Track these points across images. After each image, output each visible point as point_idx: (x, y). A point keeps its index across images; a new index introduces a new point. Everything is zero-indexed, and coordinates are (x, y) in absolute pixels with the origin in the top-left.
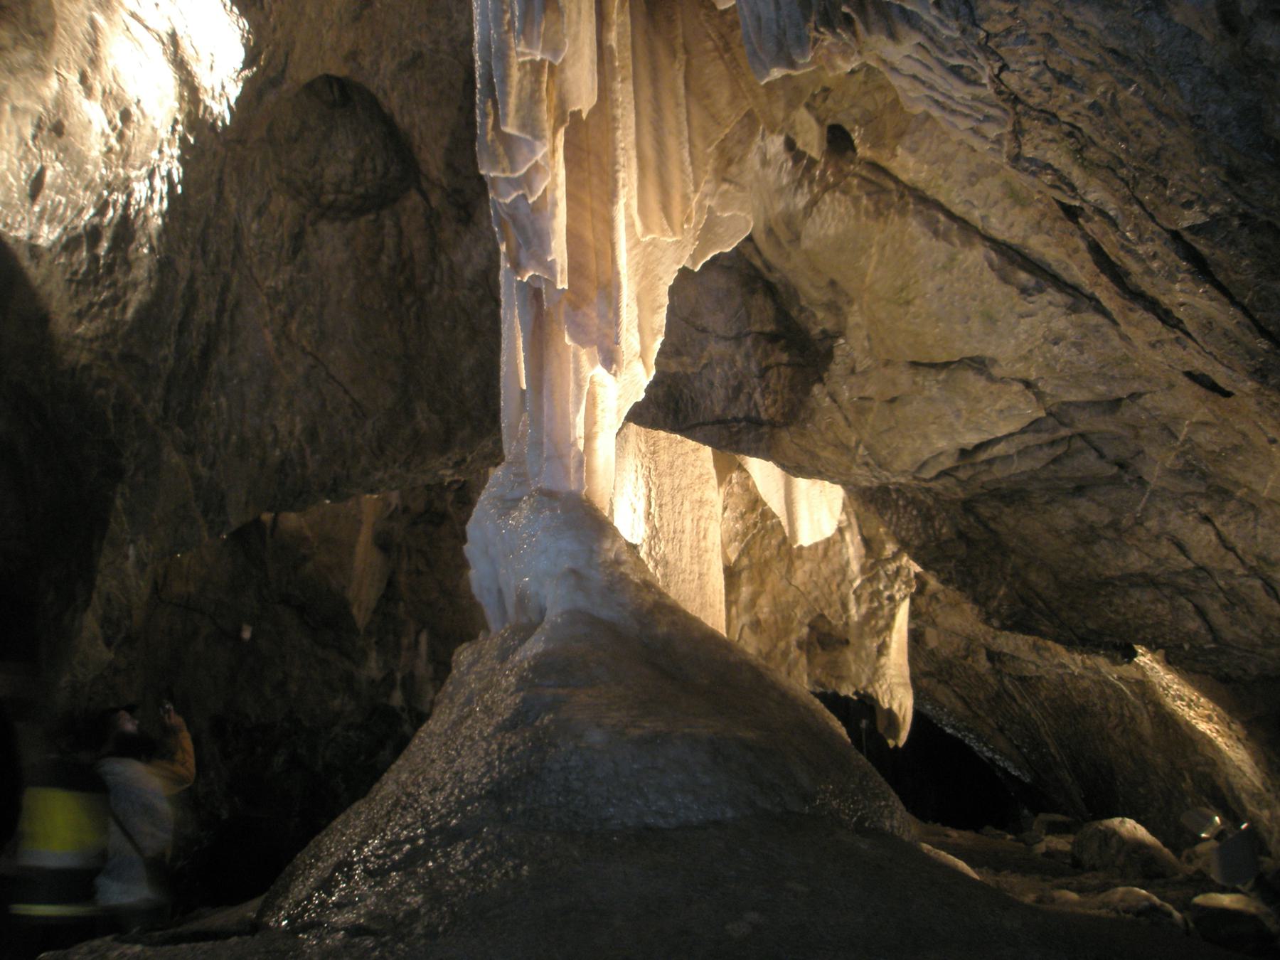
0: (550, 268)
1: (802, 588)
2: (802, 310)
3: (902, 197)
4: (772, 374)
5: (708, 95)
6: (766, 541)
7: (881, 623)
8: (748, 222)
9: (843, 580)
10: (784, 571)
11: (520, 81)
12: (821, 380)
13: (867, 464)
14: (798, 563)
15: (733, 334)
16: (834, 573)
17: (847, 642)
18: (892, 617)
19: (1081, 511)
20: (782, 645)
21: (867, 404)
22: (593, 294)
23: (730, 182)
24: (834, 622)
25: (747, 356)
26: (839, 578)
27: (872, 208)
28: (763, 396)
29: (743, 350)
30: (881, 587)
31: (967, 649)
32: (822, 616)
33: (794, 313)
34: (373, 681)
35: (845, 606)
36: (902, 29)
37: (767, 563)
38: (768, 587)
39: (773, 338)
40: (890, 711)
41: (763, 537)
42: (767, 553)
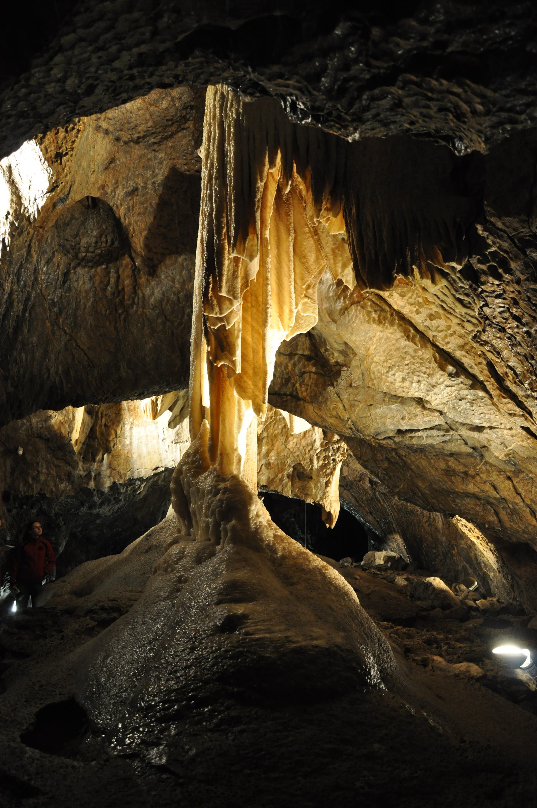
0: (234, 363)
1: (292, 450)
2: (326, 350)
3: (392, 315)
4: (307, 376)
5: (304, 257)
6: (276, 426)
7: (329, 471)
8: (315, 321)
9: (312, 449)
10: (284, 441)
11: (229, 265)
12: (332, 385)
13: (351, 429)
14: (291, 438)
15: (288, 352)
17: (311, 478)
18: (334, 469)
19: (450, 463)
20: (280, 476)
21: (356, 403)
22: (250, 372)
23: (309, 298)
24: (305, 468)
25: (295, 365)
26: (310, 447)
27: (377, 318)
28: (300, 385)
29: (292, 362)
30: (330, 454)
31: (361, 477)
32: (300, 464)
33: (322, 350)
34: (81, 476)
35: (311, 461)
36: (438, 277)
37: (275, 436)
38: (275, 448)
39: (308, 358)
40: (329, 513)
41: (275, 424)
42: (276, 432)
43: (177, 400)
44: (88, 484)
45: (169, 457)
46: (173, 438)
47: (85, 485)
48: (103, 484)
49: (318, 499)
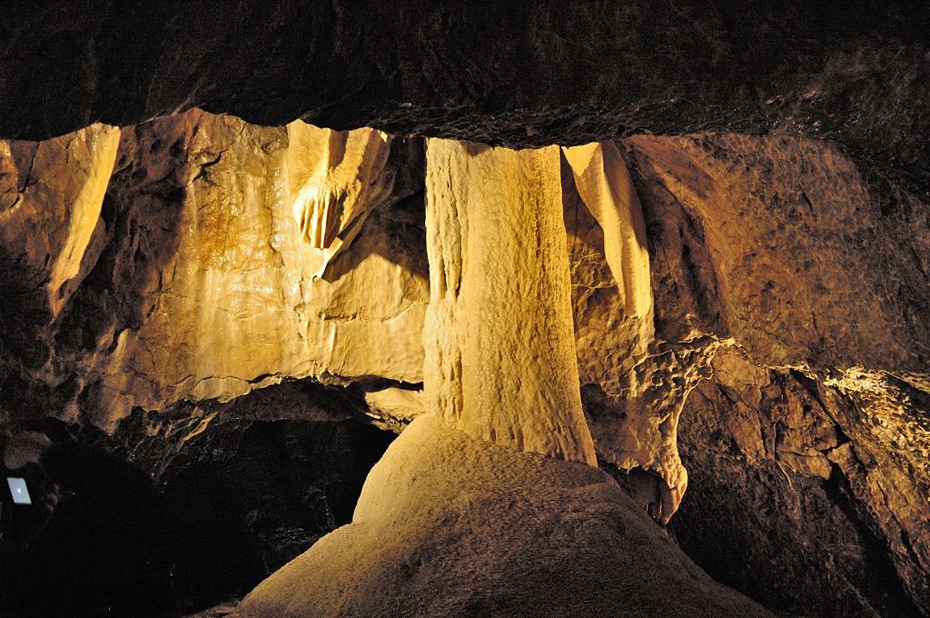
7: (665, 403)
16: (618, 347)
17: (624, 416)
26: (623, 352)
34: (46, 387)
35: (624, 381)
43: (361, 214)
44: (61, 410)
45: (306, 350)
46: (325, 304)
47: (53, 414)
48: (105, 413)
49: (652, 461)
